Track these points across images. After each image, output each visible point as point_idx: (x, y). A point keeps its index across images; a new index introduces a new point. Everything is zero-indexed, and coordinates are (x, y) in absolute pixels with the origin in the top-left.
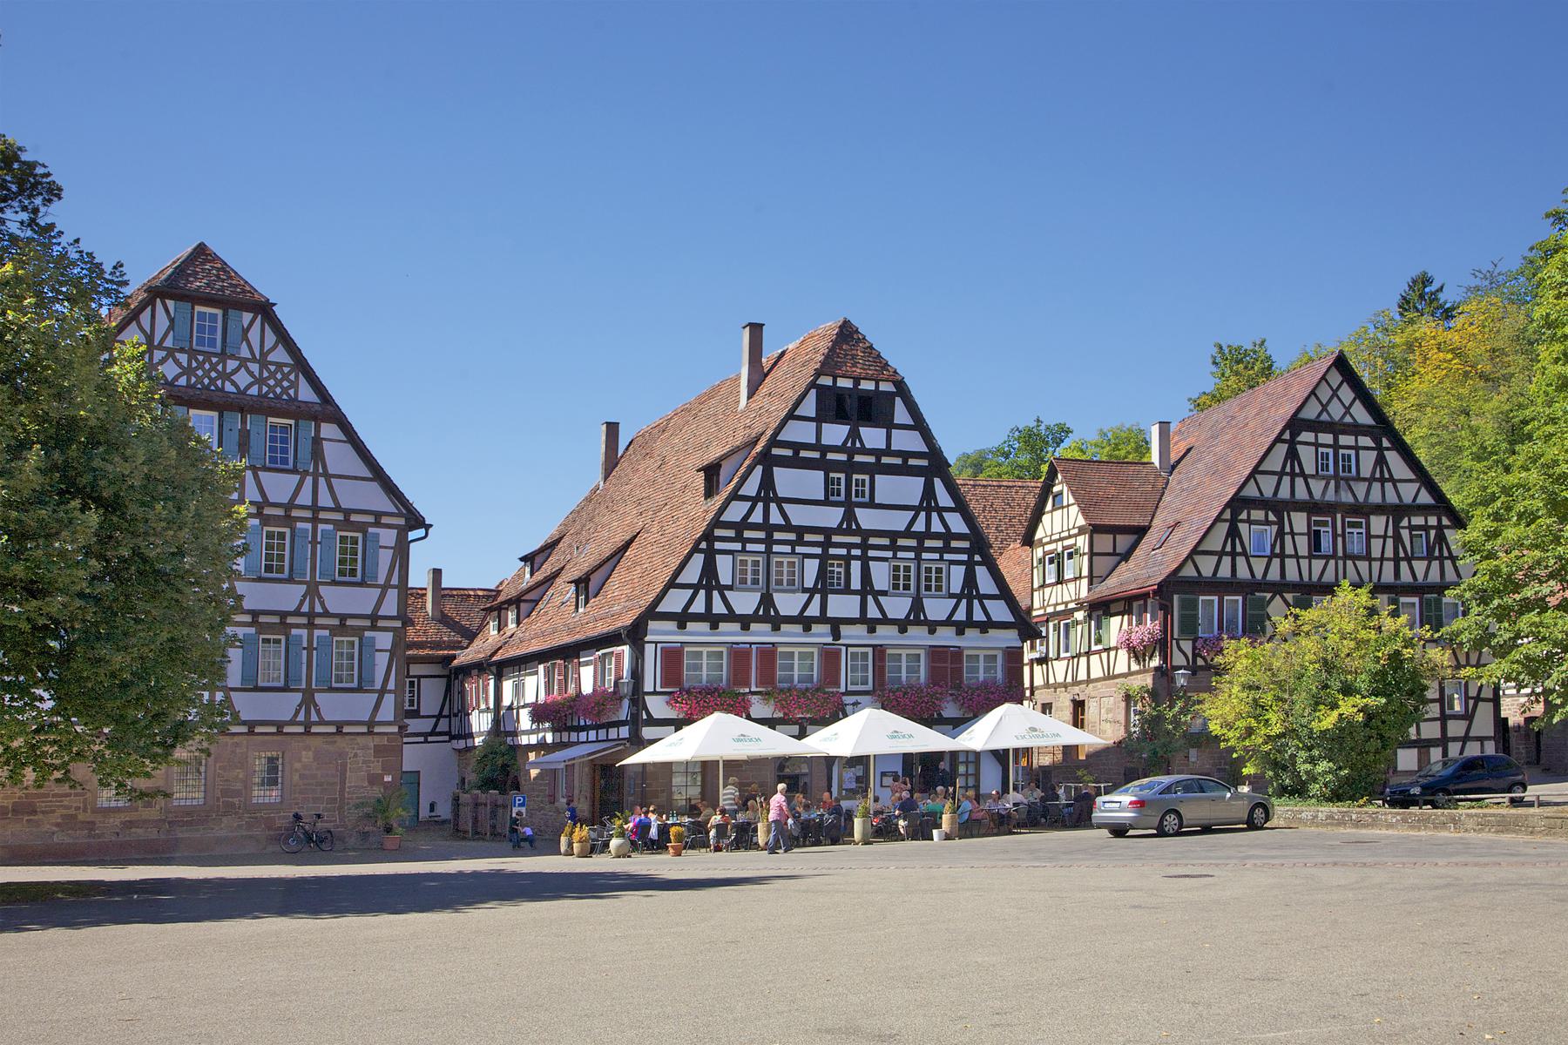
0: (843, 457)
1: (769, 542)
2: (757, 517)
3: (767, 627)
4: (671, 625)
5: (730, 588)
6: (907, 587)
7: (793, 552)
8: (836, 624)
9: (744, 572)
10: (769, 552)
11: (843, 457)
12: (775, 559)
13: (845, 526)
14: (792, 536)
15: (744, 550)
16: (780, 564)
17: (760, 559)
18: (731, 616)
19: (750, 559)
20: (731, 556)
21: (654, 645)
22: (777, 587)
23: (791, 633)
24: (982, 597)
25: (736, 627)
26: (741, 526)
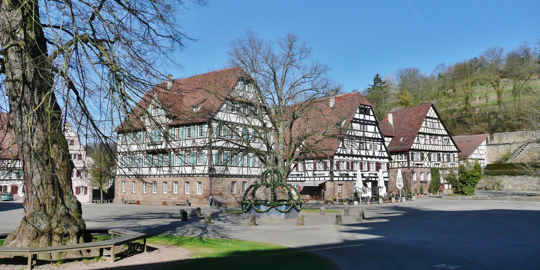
6: (372, 149)
8: (362, 157)
23: (355, 159)
24: (383, 151)
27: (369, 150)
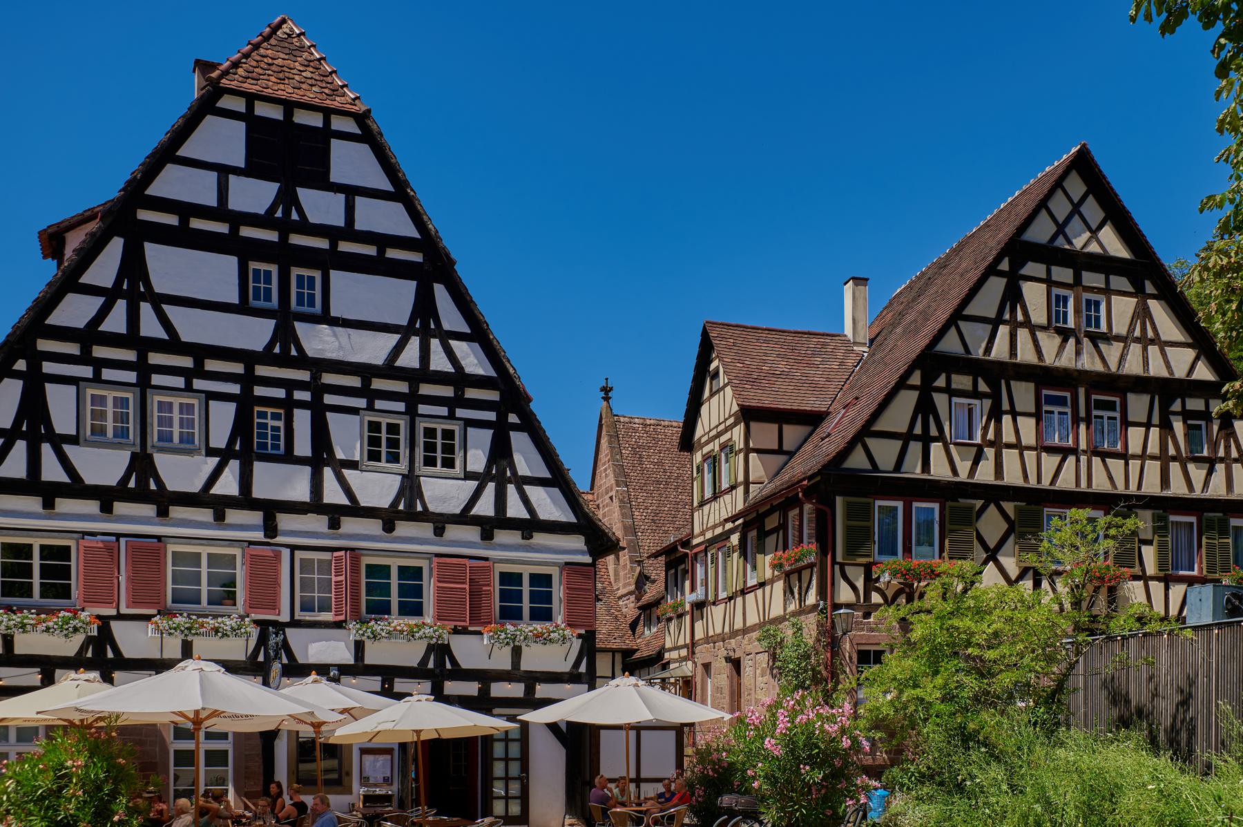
0: (272, 236)
2: (116, 322)
3: (149, 510)
5: (74, 440)
7: (189, 388)
8: (271, 509)
9: (99, 415)
10: (144, 385)
11: (272, 236)
12: (155, 399)
13: (277, 350)
14: (187, 362)
15: (97, 379)
17: (129, 395)
18: (76, 488)
19: (110, 395)
20: (74, 388)
22: (161, 444)
25: (92, 507)
26: (90, 335)
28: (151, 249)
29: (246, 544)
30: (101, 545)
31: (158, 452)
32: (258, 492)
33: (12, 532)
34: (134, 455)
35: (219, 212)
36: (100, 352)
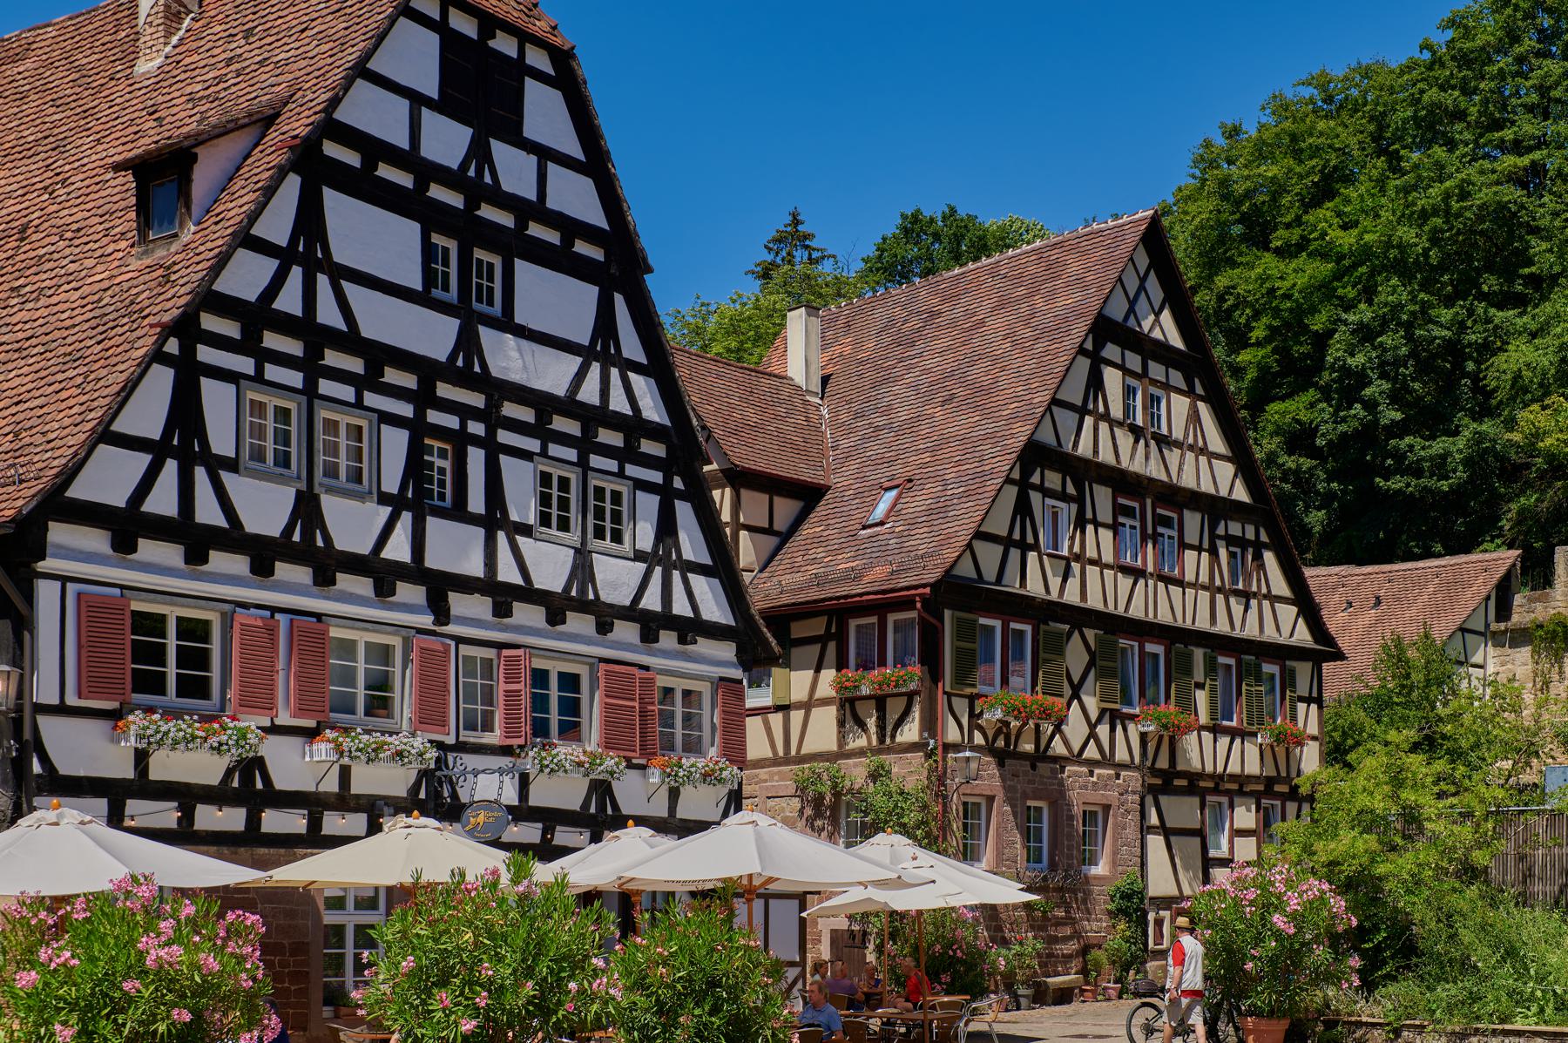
0: (455, 200)
1: (311, 367)
3: (300, 574)
4: (96, 540)
5: (233, 465)
7: (359, 404)
8: (440, 587)
9: (259, 432)
11: (455, 200)
13: (460, 363)
14: (355, 365)
15: (259, 378)
16: (332, 426)
19: (272, 401)
20: (233, 388)
21: (58, 584)
22: (327, 481)
25: (238, 564)
27: (526, 530)
28: (333, 200)
29: (413, 631)
30: (260, 623)
31: (326, 492)
32: (432, 561)
33: (152, 596)
34: (299, 493)
35: (408, 159)
36: (272, 341)
